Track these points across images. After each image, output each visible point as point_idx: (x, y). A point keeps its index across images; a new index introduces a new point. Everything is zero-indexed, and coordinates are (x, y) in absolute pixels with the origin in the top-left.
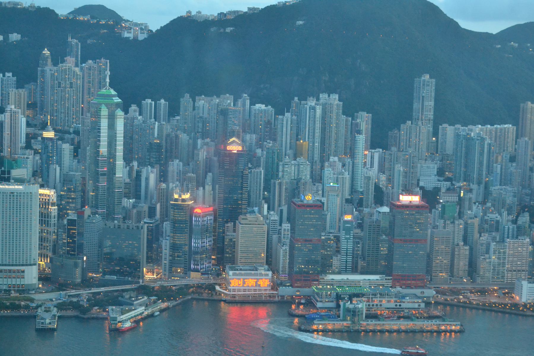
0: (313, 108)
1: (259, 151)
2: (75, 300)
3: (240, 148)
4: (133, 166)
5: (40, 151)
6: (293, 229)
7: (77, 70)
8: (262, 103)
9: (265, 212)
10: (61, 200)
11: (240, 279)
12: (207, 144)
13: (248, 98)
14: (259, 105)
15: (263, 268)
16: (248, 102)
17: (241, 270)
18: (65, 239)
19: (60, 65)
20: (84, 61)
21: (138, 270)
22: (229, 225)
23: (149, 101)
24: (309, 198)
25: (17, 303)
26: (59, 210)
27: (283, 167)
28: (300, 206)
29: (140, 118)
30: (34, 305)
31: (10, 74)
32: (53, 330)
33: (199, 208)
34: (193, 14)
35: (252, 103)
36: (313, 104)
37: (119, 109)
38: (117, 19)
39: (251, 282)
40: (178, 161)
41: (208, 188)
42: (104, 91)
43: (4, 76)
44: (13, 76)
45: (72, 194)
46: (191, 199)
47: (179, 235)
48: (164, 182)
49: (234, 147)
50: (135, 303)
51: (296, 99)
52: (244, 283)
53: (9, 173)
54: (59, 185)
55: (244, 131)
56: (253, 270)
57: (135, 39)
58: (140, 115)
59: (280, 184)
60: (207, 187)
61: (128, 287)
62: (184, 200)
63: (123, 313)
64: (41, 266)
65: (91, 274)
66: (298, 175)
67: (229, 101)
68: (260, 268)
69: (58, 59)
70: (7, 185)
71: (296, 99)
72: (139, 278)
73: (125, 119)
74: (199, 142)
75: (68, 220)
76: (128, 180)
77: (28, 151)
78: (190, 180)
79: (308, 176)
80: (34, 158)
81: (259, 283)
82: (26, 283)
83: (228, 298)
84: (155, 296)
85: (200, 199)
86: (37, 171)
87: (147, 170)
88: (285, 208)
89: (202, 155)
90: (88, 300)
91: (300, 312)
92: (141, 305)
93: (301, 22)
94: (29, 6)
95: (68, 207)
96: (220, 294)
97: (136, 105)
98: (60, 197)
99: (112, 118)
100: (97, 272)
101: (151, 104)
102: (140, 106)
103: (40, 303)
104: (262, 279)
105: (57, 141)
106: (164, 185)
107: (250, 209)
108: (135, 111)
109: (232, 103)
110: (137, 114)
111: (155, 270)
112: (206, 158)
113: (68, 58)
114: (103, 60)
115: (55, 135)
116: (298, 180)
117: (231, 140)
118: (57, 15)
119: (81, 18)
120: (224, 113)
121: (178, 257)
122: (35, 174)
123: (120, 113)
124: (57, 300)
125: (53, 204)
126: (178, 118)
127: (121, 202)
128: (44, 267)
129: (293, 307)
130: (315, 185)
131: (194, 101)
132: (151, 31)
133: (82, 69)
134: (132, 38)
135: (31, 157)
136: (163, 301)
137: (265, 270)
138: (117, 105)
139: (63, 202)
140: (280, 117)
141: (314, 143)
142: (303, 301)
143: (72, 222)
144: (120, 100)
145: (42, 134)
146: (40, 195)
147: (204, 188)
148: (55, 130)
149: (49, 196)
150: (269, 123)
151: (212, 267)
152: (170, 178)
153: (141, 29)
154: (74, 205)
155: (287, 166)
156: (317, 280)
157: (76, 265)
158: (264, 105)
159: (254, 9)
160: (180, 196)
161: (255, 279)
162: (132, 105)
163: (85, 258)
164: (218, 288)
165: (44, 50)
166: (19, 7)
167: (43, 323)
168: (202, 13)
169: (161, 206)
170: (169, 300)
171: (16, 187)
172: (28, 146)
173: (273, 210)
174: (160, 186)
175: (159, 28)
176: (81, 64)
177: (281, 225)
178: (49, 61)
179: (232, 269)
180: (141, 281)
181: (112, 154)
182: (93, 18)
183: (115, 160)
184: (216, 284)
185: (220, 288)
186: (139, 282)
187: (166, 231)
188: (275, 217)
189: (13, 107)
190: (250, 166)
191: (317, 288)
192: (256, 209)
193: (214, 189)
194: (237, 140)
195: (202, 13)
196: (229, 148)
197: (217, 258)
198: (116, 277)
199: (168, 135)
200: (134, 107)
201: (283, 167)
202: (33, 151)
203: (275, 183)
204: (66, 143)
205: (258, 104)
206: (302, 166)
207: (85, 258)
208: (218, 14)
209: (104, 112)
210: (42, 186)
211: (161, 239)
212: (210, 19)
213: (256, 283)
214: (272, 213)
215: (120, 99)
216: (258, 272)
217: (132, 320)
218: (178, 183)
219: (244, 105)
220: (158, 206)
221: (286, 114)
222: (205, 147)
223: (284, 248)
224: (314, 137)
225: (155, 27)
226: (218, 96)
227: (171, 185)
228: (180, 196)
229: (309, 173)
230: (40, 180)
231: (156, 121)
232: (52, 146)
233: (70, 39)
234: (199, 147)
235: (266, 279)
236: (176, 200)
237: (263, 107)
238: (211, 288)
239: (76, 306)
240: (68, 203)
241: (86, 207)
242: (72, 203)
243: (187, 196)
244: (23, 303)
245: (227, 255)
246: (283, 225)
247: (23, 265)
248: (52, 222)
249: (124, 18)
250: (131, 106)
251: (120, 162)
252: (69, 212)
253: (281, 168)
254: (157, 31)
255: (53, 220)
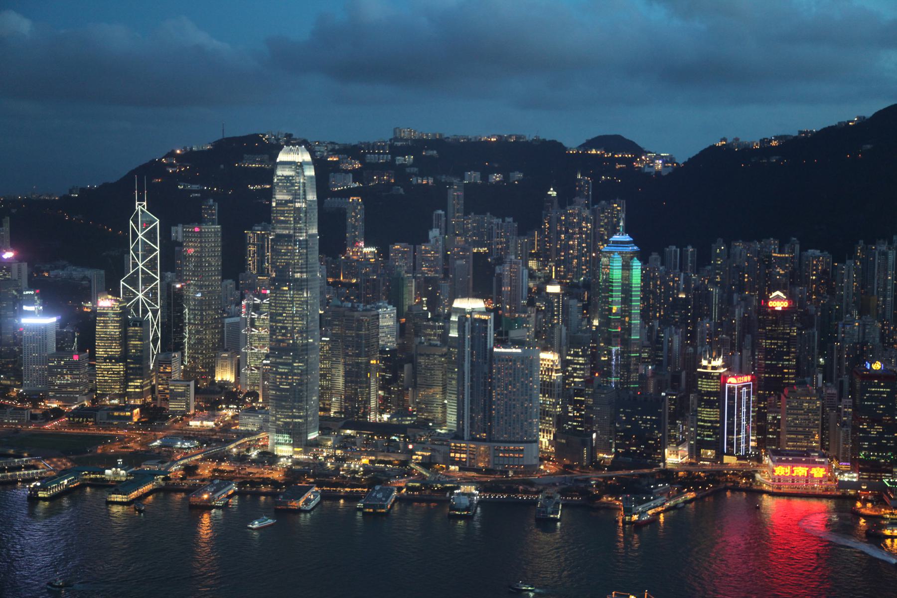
0: (884, 254)
1: (812, 309)
2: (583, 485)
3: (786, 304)
4: (653, 326)
5: (543, 308)
6: (854, 406)
7: (586, 213)
8: (816, 248)
9: (820, 384)
10: (568, 366)
11: (785, 466)
12: (744, 299)
13: (798, 242)
14: (812, 251)
15: (817, 454)
16: (797, 247)
17: (788, 455)
18: (570, 412)
19: (568, 208)
20: (596, 200)
21: (658, 451)
22: (772, 398)
23: (674, 248)
24: (877, 366)
25: (515, 487)
26: (565, 378)
27: (843, 327)
28: (864, 377)
29: (661, 268)
30: (534, 490)
31: (511, 220)
32: (556, 520)
33: (733, 376)
34: (729, 141)
35: (804, 249)
36: (884, 248)
37: (635, 259)
38: (638, 151)
39: (801, 471)
40: (708, 320)
41: (747, 353)
42: (616, 238)
43: (503, 221)
44: (514, 221)
45: (580, 359)
46: (723, 366)
47: (709, 410)
48: (690, 345)
49: (778, 302)
50: (654, 491)
51: (861, 242)
52: (793, 472)
53: (507, 334)
54: (564, 348)
55: (791, 283)
56: (803, 456)
57: (658, 173)
58: (662, 264)
59: (840, 349)
60: (744, 352)
61: (646, 471)
62: (714, 368)
63: (640, 502)
64: (544, 444)
65: (601, 455)
66: (864, 338)
67: (773, 247)
68: (812, 454)
69: (565, 199)
70: (504, 348)
71: (861, 242)
72: (660, 461)
73: (642, 270)
74: (736, 297)
75: (575, 389)
76: (647, 343)
77: (529, 309)
78: (722, 342)
79: (877, 339)
80: (536, 317)
81: (812, 472)
82: (525, 463)
83: (771, 489)
84: (679, 483)
85: (737, 367)
86: (540, 332)
87: (671, 331)
88: (846, 378)
89: (738, 312)
90: (598, 485)
91: (868, 512)
92: (662, 494)
93: (869, 146)
94: (533, 140)
95: (575, 375)
96: (761, 484)
97: (657, 253)
98: (565, 363)
99: (627, 267)
100: (609, 453)
101: (676, 252)
102: (662, 254)
103: (541, 488)
104: (815, 467)
105: (562, 297)
106: (691, 349)
107: (800, 379)
108: (656, 260)
109: (777, 250)
110: (659, 263)
111: (680, 452)
112: (744, 316)
113: (577, 199)
114: (618, 200)
115: (561, 290)
116: (864, 343)
117: (774, 294)
118: (565, 149)
119: (594, 152)
120: (767, 262)
121: (708, 436)
122: (537, 334)
123: (637, 265)
124: (561, 484)
125: (557, 371)
126: (709, 268)
127: (637, 369)
128: (547, 445)
129: (859, 505)
130: (886, 350)
131: (729, 247)
132: (677, 164)
133: (594, 212)
134: (654, 172)
135: (533, 315)
136: (689, 491)
137: (821, 456)
138: (635, 254)
139: (570, 369)
140: (840, 265)
141: (885, 297)
142: (870, 497)
143: (580, 393)
144: (636, 248)
145: (546, 288)
146: (543, 360)
147: (741, 352)
148: (560, 283)
149: (552, 361)
150: (824, 272)
151: (750, 450)
152: (698, 341)
153: (664, 162)
154: (582, 372)
155: (848, 327)
156: (891, 472)
157: (584, 444)
158: (819, 251)
159: (806, 133)
160: (710, 362)
161: (807, 467)
162: (653, 253)
163: (594, 436)
164: (758, 476)
165: (549, 190)
166: (521, 140)
167: (543, 512)
168: (740, 140)
169: (687, 374)
170: (696, 490)
171: (514, 350)
172: (531, 303)
173: (831, 381)
174: (686, 350)
175: (687, 160)
176: (593, 205)
177: (840, 401)
178: (556, 202)
179: (775, 453)
180: (662, 464)
181: (626, 311)
182: (607, 152)
183: (630, 320)
184: (756, 471)
185: (762, 476)
186: (660, 466)
187: (693, 404)
188: (834, 391)
189: (513, 257)
190: (799, 325)
191: (889, 482)
192: (808, 379)
193: (753, 355)
194: (781, 294)
195: (740, 140)
196: (771, 304)
197: (758, 439)
198: (631, 459)
199: (696, 289)
200: (655, 255)
201: (843, 327)
202: (535, 309)
203: (832, 348)
204: (573, 299)
205: (811, 249)
206: (869, 327)
207: (594, 436)
208: (761, 140)
209: (618, 263)
210: (545, 349)
211: (687, 414)
212: (751, 146)
213: (808, 471)
214: (829, 384)
215: (636, 245)
216: (811, 458)
217: (650, 512)
218: (708, 346)
219: (793, 251)
220: (684, 374)
221: (848, 262)
222: (743, 303)
223: (845, 429)
224: (885, 289)
225: (682, 159)
226: (760, 241)
227: (699, 348)
228: (710, 362)
229: (878, 335)
230: (543, 342)
231: (681, 271)
232: (558, 302)
233: (579, 177)
234: (735, 303)
235: (821, 467)
236: (705, 367)
237: (818, 252)
238: (750, 475)
239: (585, 492)
240: (575, 370)
241: (597, 375)
242: (581, 369)
243: (719, 362)
244: (521, 487)
245: (771, 436)
246: (843, 400)
247: (522, 442)
248: (556, 393)
249: (645, 150)
250: (651, 255)
251: (636, 322)
252: (576, 380)
253: (840, 329)
254: (684, 163)
255: (556, 389)
